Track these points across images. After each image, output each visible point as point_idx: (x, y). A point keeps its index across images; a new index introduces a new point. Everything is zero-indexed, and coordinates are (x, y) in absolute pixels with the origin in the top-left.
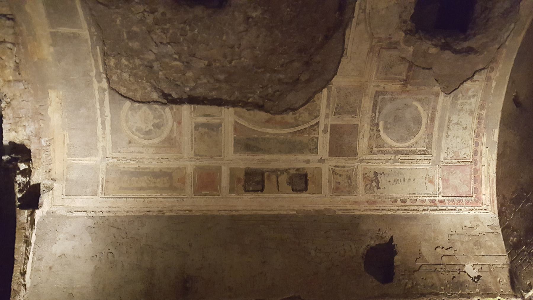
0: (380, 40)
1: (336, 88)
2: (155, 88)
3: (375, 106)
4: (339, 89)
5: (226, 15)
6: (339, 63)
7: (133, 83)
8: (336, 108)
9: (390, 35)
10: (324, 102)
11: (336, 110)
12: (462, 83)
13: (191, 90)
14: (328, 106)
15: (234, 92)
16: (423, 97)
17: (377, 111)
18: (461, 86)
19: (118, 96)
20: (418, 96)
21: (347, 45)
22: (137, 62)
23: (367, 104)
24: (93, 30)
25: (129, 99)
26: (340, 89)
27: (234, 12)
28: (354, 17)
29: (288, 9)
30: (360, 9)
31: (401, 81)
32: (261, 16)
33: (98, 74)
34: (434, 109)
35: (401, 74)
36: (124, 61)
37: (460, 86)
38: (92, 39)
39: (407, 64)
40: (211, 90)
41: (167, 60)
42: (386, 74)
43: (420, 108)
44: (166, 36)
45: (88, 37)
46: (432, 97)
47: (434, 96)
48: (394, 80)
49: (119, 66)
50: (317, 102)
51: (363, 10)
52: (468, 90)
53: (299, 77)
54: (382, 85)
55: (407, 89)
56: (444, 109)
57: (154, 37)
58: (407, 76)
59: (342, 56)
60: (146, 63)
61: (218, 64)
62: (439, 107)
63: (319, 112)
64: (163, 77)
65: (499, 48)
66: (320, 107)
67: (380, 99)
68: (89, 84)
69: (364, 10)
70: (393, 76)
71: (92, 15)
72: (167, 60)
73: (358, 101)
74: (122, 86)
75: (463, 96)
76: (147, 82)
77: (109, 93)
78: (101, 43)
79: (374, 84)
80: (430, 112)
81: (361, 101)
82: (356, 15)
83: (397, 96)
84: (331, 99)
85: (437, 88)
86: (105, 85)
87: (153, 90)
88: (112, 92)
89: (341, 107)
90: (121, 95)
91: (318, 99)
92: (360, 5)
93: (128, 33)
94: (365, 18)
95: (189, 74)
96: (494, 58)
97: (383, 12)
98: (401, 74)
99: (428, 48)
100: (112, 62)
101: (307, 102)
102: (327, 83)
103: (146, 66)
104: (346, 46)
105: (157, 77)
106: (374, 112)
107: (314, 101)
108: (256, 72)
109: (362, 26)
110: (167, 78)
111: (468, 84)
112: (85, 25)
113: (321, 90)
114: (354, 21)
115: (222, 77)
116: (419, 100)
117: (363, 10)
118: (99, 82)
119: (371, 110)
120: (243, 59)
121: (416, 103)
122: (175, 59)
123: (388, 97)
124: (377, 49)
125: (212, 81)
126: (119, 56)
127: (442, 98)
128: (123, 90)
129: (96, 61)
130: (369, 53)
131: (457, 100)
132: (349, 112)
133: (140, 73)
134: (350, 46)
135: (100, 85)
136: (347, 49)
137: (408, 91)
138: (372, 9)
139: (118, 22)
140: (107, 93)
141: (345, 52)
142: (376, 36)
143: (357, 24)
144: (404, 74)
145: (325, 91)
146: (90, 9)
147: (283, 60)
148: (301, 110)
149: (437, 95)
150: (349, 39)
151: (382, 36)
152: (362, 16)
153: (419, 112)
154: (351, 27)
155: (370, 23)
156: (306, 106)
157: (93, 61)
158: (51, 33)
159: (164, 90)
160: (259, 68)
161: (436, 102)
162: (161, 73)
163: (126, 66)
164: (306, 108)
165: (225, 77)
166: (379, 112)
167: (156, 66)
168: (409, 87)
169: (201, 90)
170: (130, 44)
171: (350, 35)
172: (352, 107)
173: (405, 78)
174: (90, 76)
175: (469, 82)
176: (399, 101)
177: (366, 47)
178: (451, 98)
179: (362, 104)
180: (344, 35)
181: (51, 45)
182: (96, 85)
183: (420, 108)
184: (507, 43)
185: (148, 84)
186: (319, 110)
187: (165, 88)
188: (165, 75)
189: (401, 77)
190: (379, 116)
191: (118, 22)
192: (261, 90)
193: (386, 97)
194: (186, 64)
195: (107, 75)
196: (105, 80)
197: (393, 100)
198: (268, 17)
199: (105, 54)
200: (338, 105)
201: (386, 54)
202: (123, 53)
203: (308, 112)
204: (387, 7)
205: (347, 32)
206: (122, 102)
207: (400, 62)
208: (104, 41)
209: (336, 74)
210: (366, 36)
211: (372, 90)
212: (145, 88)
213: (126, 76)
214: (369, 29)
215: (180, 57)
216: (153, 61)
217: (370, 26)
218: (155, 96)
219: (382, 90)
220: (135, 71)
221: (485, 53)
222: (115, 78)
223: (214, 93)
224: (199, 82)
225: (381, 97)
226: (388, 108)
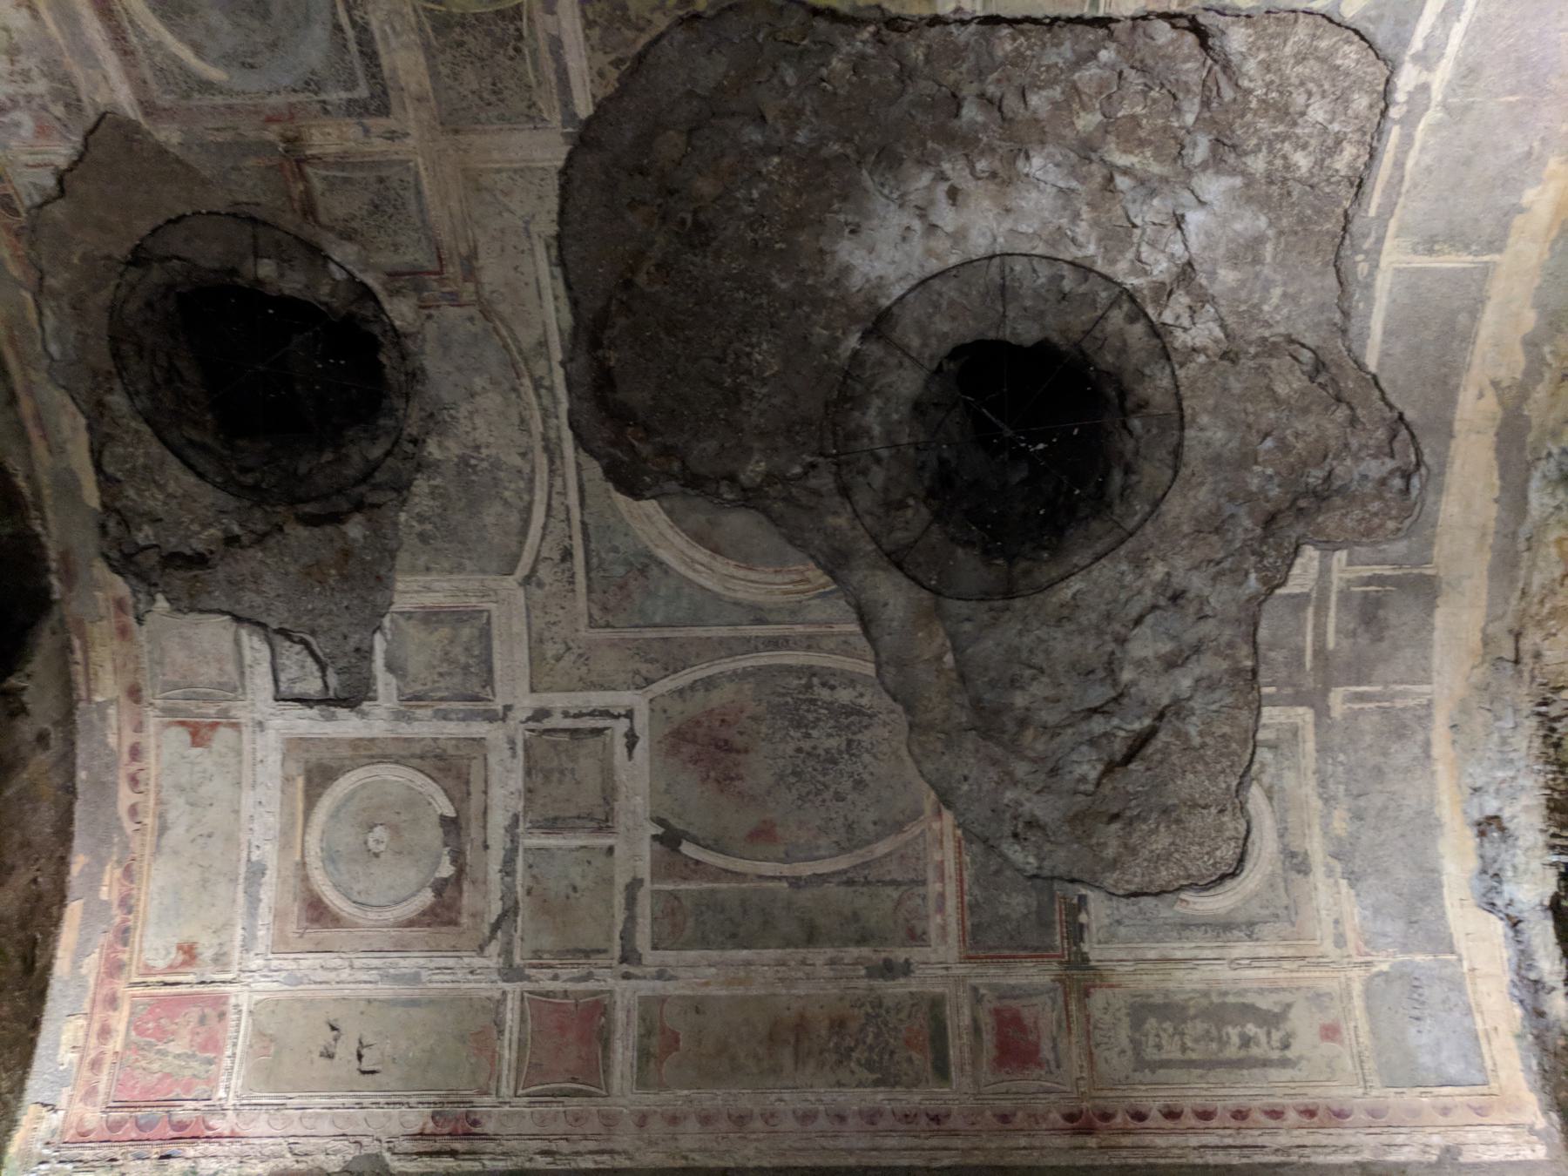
0: (454, 299)
1: (543, 120)
2: (1226, 67)
3: (370, 56)
4: (533, 117)
5: (946, 335)
6: (562, 212)
7: (1302, 84)
8: (520, 37)
9: (429, 317)
10: (577, 62)
11: (518, 30)
12: (81, 157)
13: (1093, 55)
14: (556, 45)
15: (927, 61)
16: (198, 100)
17: (350, 33)
18: (79, 147)
19: (1380, 36)
20: (219, 100)
21: (553, 277)
22: (1257, 164)
23: (405, 62)
24: (1363, 268)
25: (1339, 25)
26: (531, 118)
27: (925, 345)
28: (563, 364)
29: (759, 358)
30: (551, 389)
31: (313, 157)
32: (839, 333)
33: (1409, 121)
34: (125, 53)
35: (331, 184)
36: (1303, 161)
37: (86, 145)
38: (1380, 240)
39: (323, 219)
40: (1018, 59)
41: (1156, 169)
42: (381, 180)
43: (186, 54)
44: (1138, 253)
45: (1388, 245)
46: (165, 100)
47: (159, 103)
48: (342, 161)
49: (1330, 142)
50: (603, 60)
51: (542, 386)
52: (42, 131)
53: (689, 143)
54: (379, 145)
55: (275, 127)
56: (87, 55)
57: (1178, 249)
58: (304, 177)
59: (559, 237)
60: (1231, 158)
61: (982, 165)
62: (111, 63)
63: (584, 15)
64: (1185, 106)
65: (41, 279)
66: (587, 38)
67: (362, 82)
68: (1469, 72)
69: (537, 385)
70: (358, 175)
71: (1346, 314)
72: (1156, 169)
73: (444, 71)
74: (1347, 74)
75: (44, 108)
76: (1249, 92)
77: (1405, 44)
78: (1354, 228)
79: (411, 142)
80: (134, 40)
81: (434, 75)
82: (559, 375)
83: (301, 97)
84: (553, 77)
85: (168, 135)
86: (1407, 79)
87: (1235, 59)
88: (1389, 52)
89: (502, 43)
90: (1363, 38)
91: (601, 74)
92: (556, 402)
93: (1257, 260)
94: (526, 364)
95: (1087, 121)
96: (32, 244)
97: (479, 382)
98: (331, 184)
99: (282, 276)
100: (1349, 154)
101: (640, 58)
102: (586, 139)
103: (1234, 147)
104: (558, 271)
105: (1206, 104)
106: (363, 30)
107: (616, 64)
108: (849, 140)
109: (528, 338)
110: (1175, 97)
111: (61, 153)
112: (1383, 283)
113: (601, 107)
114: (557, 355)
115: (971, 112)
116: (207, 86)
117: (542, 386)
118: (1424, 88)
119: (377, 36)
120: (895, 196)
121: (216, 74)
122: (1126, 171)
123: (336, 96)
124: (451, 269)
125: (1011, 103)
126: (1315, 180)
127: (123, 97)
128: (1350, 55)
129: (1399, 165)
130: (474, 254)
131: (57, 95)
132: (463, 26)
133: (1262, 124)
134: (542, 268)
135: (1425, 77)
136: (551, 264)
137: (270, 120)
138: (514, 389)
139: (1277, 292)
140: (1417, 44)
141: (554, 252)
142: (474, 311)
143: (543, 344)
144: (318, 186)
145: (584, 108)
146: (1344, 332)
147: (755, 194)
148: (661, 23)
149: (148, 108)
150: (556, 298)
151: (452, 312)
152: (540, 368)
153: (181, 40)
154: (562, 340)
155: (506, 346)
156: (644, 39)
157: (1410, 164)
158: (1500, 250)
159: (1197, 51)
160: (838, 157)
161: (139, 85)
162: (1190, 119)
163: (1304, 147)
164: (641, 30)
165: (957, 115)
166: (338, 28)
167: (1200, 150)
168: (272, 134)
169: (1054, 59)
170: (1263, 222)
171: (557, 310)
172: (461, 44)
173: (309, 170)
174: (1445, 106)
175: (63, 163)
176: (287, 81)
177: (492, 272)
178: (84, 98)
179: (422, 59)
180: (575, 304)
181: (1521, 210)
182: (1440, 78)
183: (186, 54)
184: (28, 296)
185: (1245, 83)
186: (589, 24)
187: (1187, 59)
188: (1178, 110)
189: (324, 173)
190: (334, 14)
191: (1277, 292)
192: (824, 72)
193: (344, 95)
194: (1093, 156)
195: (1384, 113)
196: (1400, 96)
197: (312, 84)
198: (818, 329)
199: (1359, 185)
200: (517, 50)
201: (415, 255)
202: (1297, 189)
203: (632, 14)
204: (472, 396)
205: (567, 319)
206: (1373, 13)
207: (354, 224)
208: (1344, 229)
209: (563, 172)
210: (504, 308)
211: (411, 119)
212: (1266, 67)
213: (1318, 112)
214: (504, 332)
215: (1111, 179)
216: (1204, 166)
217: (502, 338)
218: (1237, 39)
219: (368, 121)
220: (1280, 128)
221: (76, 261)
222: (1361, 102)
223: (1008, 47)
224: (1056, 93)
225: (362, 92)
226: (313, 50)
